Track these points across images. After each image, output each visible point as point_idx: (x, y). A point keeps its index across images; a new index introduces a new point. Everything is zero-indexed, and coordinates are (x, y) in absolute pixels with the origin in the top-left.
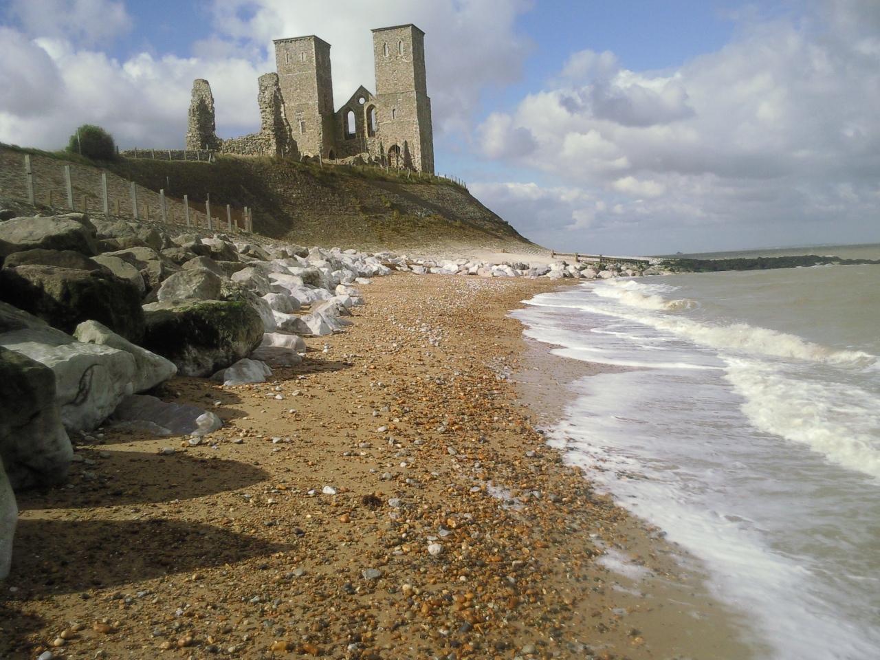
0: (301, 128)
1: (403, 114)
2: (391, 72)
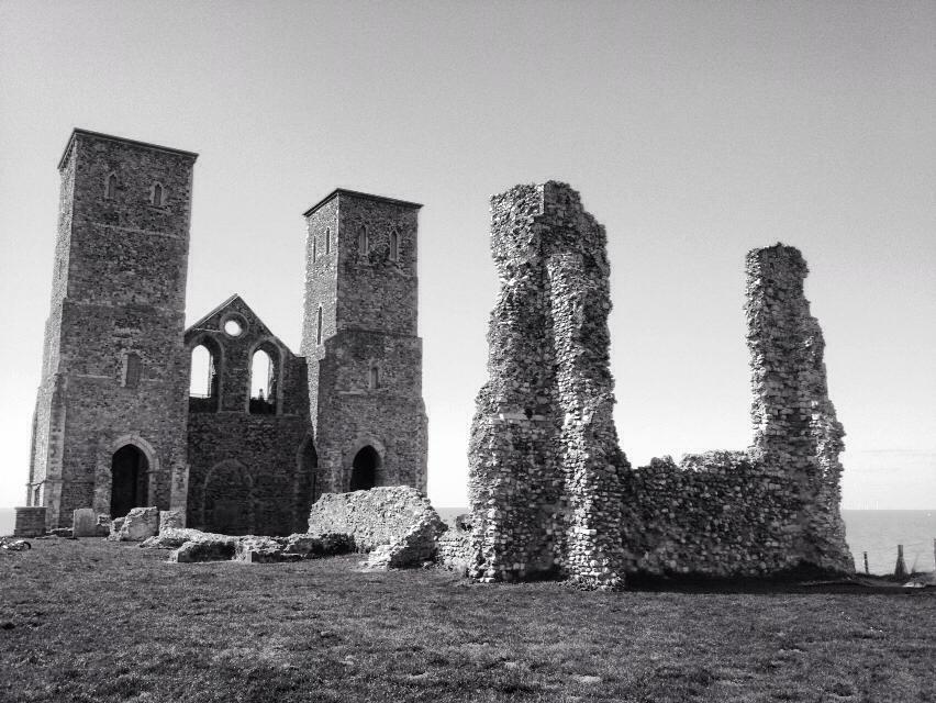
0: (124, 370)
1: (394, 381)
2: (371, 287)
